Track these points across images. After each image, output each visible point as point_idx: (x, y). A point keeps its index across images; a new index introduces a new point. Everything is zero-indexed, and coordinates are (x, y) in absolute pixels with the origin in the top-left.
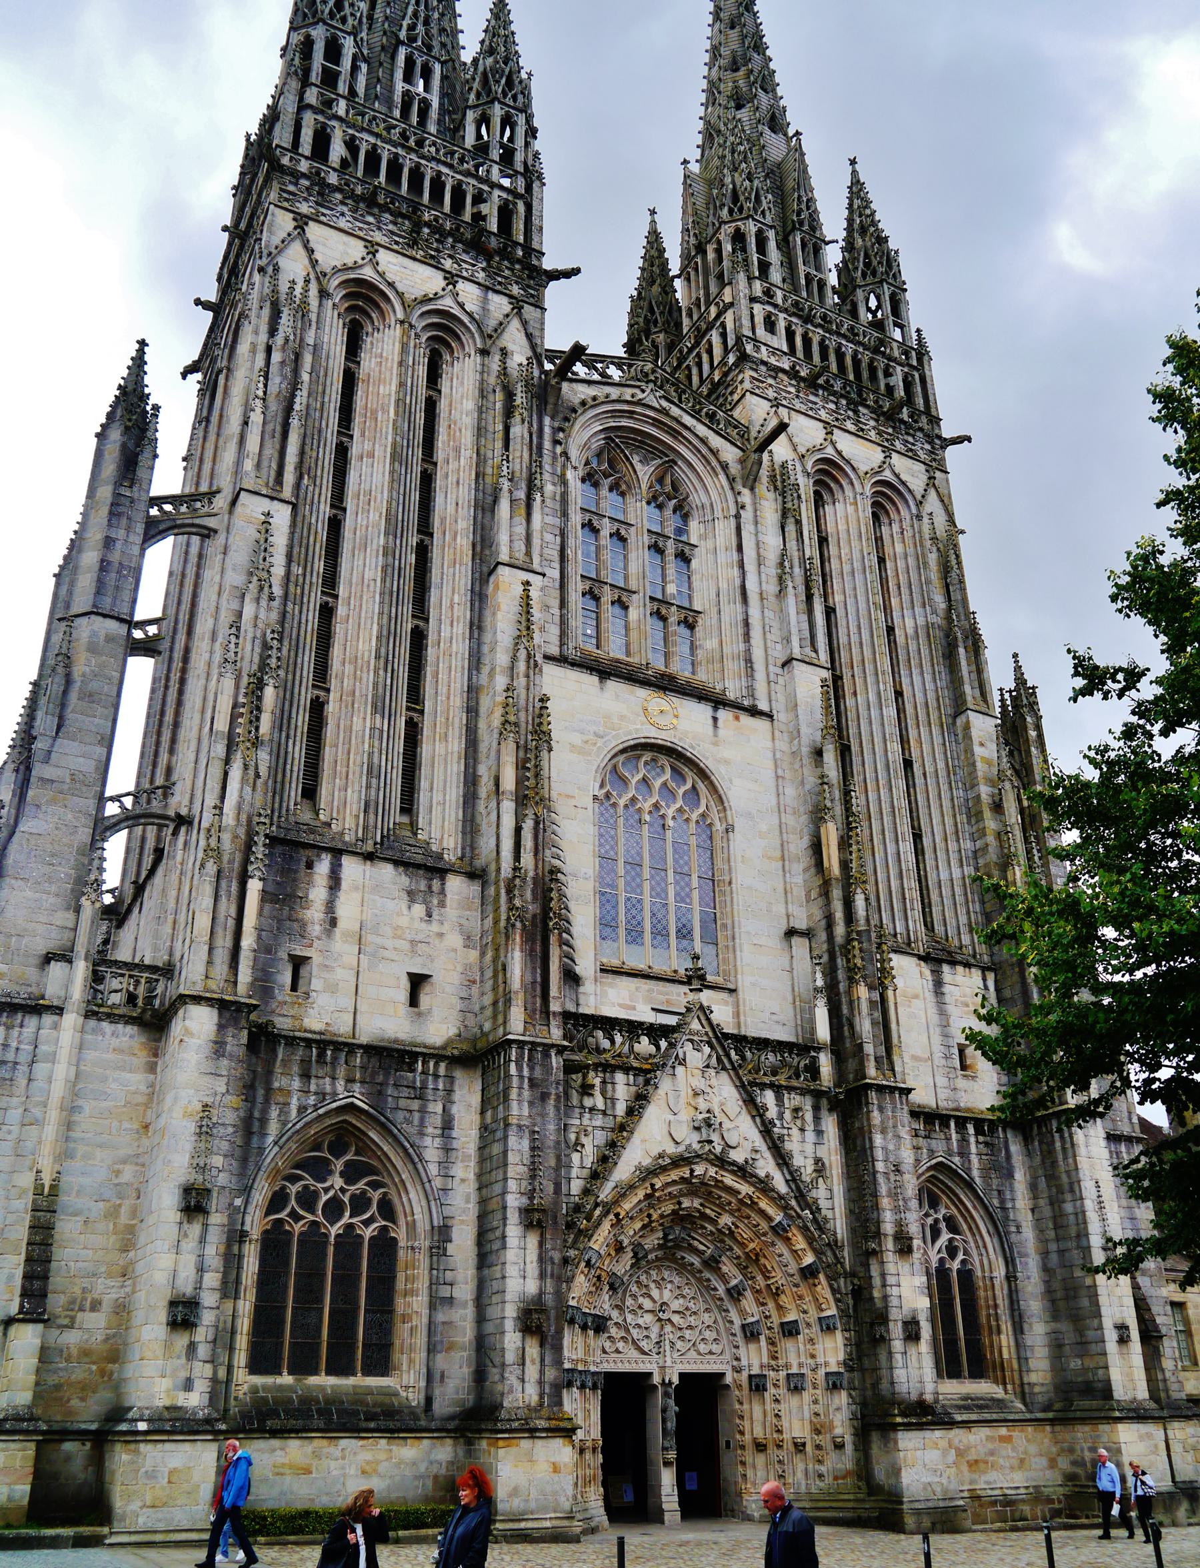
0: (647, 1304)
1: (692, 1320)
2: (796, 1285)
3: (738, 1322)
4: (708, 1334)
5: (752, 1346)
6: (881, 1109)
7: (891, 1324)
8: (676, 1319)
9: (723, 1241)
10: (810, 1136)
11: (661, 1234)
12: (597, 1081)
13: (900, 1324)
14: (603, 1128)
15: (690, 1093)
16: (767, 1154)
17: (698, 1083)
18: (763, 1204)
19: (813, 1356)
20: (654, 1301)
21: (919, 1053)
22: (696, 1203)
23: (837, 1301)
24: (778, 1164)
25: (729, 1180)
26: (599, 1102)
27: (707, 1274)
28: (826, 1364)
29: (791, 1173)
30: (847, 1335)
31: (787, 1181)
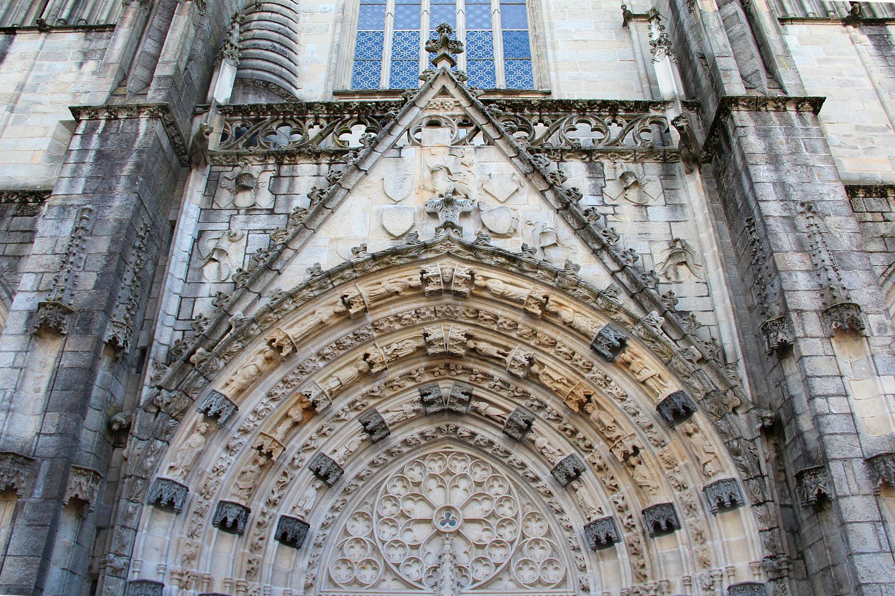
0: (420, 511)
1: (507, 534)
2: (660, 444)
3: (578, 524)
4: (539, 554)
5: (608, 564)
6: (765, 134)
7: (836, 469)
8: (474, 532)
9: (525, 395)
10: (658, 213)
11: (415, 395)
12: (266, 178)
13: (859, 466)
14: (265, 231)
15: (427, 173)
16: (575, 243)
17: (442, 158)
18: (570, 312)
19: (705, 563)
20: (433, 508)
21: (869, 123)
22: (456, 331)
23: (735, 453)
24: (595, 252)
25: (498, 281)
26: (265, 200)
27: (519, 455)
28: (732, 571)
29: (615, 259)
30: (761, 510)
31: (613, 274)
